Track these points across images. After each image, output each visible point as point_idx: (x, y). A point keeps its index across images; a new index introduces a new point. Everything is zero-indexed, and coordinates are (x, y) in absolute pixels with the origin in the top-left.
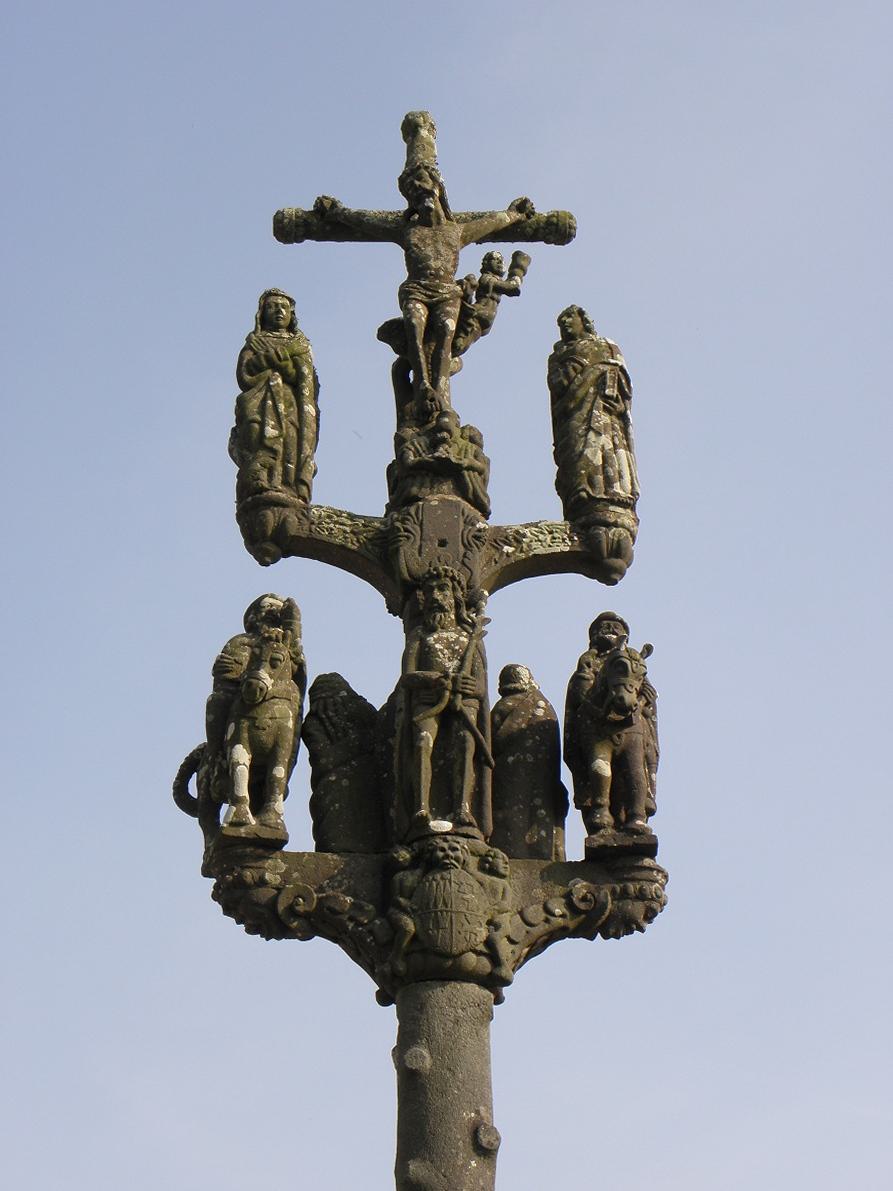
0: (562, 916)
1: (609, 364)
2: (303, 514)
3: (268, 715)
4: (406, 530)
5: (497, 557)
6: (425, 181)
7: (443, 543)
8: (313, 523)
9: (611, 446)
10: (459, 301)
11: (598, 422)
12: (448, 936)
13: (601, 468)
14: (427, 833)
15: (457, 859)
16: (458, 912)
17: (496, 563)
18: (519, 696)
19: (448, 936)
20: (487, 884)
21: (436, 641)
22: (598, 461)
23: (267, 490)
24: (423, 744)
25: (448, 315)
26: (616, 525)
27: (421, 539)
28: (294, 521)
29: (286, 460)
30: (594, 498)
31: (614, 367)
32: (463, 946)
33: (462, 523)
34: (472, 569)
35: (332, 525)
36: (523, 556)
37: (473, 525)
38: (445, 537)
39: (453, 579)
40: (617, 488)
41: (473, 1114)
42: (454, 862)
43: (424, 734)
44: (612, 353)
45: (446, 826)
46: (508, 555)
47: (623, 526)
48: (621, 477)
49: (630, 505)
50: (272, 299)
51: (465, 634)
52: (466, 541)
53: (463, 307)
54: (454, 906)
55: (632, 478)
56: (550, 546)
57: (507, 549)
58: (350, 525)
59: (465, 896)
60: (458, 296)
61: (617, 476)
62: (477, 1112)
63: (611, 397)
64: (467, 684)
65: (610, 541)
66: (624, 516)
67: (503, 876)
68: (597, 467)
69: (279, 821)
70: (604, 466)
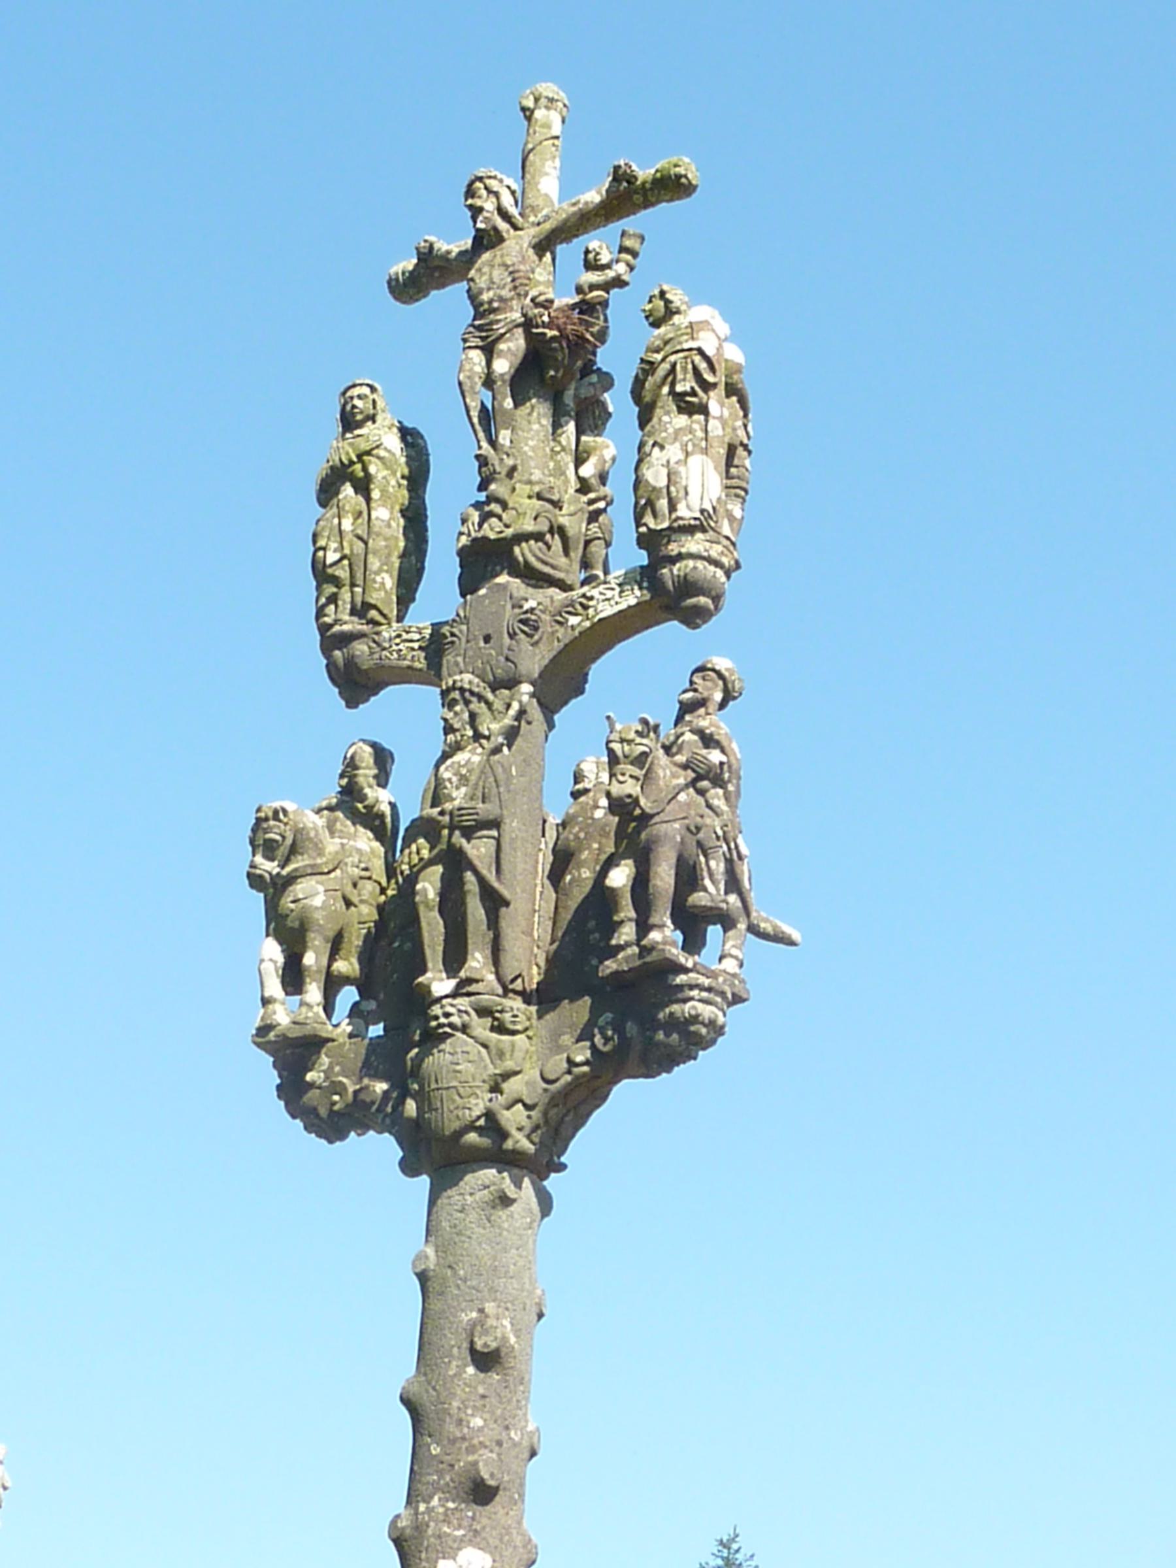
0: (587, 1063)
1: (683, 350)
2: (374, 641)
3: (291, 899)
4: (453, 635)
6: (480, 197)
7: (487, 639)
8: (384, 649)
9: (682, 456)
10: (520, 330)
11: (666, 431)
12: (439, 1119)
13: (665, 491)
14: (430, 1000)
15: (451, 1025)
16: (448, 1088)
17: (559, 641)
18: (582, 799)
19: (439, 1116)
20: (492, 1045)
21: (447, 769)
22: (662, 482)
23: (331, 626)
25: (501, 354)
26: (680, 557)
27: (468, 641)
28: (363, 652)
29: (353, 585)
30: (655, 531)
31: (686, 353)
32: (456, 1125)
33: (509, 606)
34: (515, 661)
35: (401, 647)
36: (587, 624)
37: (521, 607)
38: (490, 631)
39: (462, 690)
40: (682, 511)
41: (474, 1315)
42: (447, 1030)
43: (419, 887)
44: (692, 334)
46: (573, 627)
47: (691, 556)
49: (695, 526)
50: (349, 394)
51: (480, 750)
52: (511, 631)
53: (529, 336)
54: (444, 1081)
55: (703, 493)
56: (617, 603)
57: (574, 620)
58: (418, 641)
59: (458, 1068)
60: (518, 326)
61: (682, 493)
62: (481, 1311)
63: (685, 394)
64: (462, 815)
65: (676, 579)
69: (310, 1014)
70: (668, 487)
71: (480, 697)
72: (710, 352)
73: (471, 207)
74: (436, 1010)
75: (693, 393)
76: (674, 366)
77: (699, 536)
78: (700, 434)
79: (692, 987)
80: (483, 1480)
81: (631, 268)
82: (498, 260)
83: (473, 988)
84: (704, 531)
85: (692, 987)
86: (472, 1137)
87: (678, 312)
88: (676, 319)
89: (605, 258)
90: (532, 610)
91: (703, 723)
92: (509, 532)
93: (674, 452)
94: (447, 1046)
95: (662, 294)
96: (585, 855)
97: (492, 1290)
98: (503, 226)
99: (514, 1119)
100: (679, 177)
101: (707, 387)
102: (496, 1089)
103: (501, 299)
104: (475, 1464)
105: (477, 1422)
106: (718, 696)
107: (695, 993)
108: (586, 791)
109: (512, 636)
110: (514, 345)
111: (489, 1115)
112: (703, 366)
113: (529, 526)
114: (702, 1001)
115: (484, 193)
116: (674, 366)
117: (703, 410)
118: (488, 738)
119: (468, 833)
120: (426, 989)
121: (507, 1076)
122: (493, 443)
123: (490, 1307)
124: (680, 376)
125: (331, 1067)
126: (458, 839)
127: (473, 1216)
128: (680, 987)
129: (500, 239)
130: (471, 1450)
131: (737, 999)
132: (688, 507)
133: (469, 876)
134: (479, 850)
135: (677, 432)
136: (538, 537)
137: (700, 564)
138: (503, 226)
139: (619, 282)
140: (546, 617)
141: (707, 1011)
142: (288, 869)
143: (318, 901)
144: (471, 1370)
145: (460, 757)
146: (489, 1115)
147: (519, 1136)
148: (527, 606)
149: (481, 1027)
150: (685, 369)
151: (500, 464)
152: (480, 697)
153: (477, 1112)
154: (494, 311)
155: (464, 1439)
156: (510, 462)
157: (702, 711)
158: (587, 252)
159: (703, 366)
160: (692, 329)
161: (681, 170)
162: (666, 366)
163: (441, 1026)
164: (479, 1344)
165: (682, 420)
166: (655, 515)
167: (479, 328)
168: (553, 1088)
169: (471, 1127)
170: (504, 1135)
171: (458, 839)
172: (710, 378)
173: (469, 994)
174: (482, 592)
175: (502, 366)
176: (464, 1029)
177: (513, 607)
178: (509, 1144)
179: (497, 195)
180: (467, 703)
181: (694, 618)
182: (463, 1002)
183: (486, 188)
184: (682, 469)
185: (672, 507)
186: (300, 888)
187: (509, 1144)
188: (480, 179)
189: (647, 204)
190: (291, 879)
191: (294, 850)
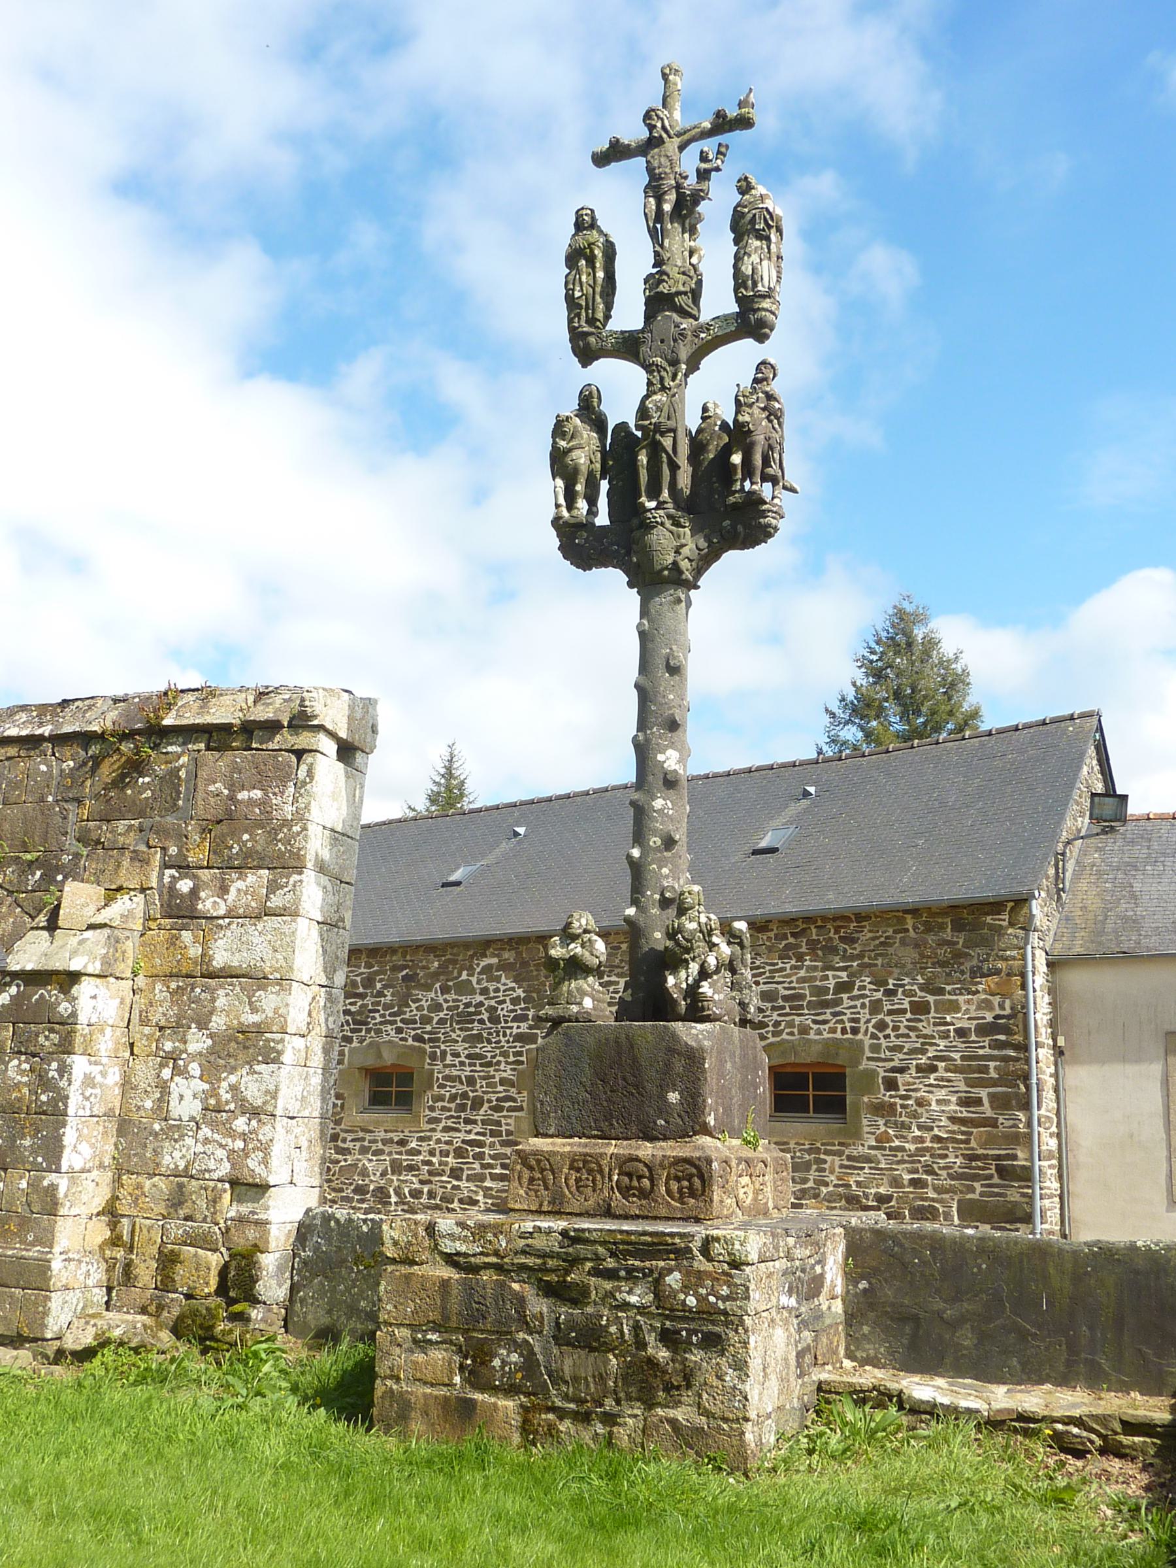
5: (696, 341)
7: (662, 341)
9: (758, 260)
15: (657, 522)
22: (749, 272)
24: (639, 463)
25: (666, 201)
26: (759, 309)
32: (660, 567)
39: (657, 365)
40: (760, 288)
45: (652, 504)
48: (762, 279)
53: (678, 193)
57: (703, 335)
62: (671, 649)
63: (760, 230)
66: (766, 304)
67: (685, 527)
68: (748, 276)
70: (752, 275)
71: (665, 369)
72: (771, 210)
73: (646, 125)
74: (648, 514)
75: (764, 230)
76: (754, 215)
77: (768, 300)
78: (766, 250)
79: (769, 511)
80: (676, 721)
81: (723, 162)
82: (663, 153)
83: (665, 506)
84: (770, 297)
85: (769, 511)
86: (666, 573)
87: (753, 188)
88: (753, 192)
89: (711, 157)
90: (685, 329)
91: (768, 389)
92: (673, 290)
93: (755, 258)
94: (655, 531)
95: (746, 178)
96: (711, 447)
97: (675, 640)
98: (665, 136)
99: (685, 565)
100: (749, 119)
101: (770, 227)
102: (677, 552)
103: (665, 173)
104: (673, 714)
105: (671, 697)
106: (771, 376)
107: (770, 514)
108: (710, 417)
109: (675, 340)
110: (672, 197)
111: (675, 563)
112: (768, 217)
113: (682, 289)
114: (773, 518)
115: (655, 118)
116: (754, 215)
117: (768, 239)
118: (670, 389)
119: (663, 434)
120: (642, 504)
121: (683, 546)
122: (662, 246)
123: (674, 647)
124: (758, 221)
125: (587, 537)
126: (658, 437)
127: (666, 608)
128: (764, 511)
129: (663, 142)
130: (669, 708)
131: (783, 517)
132: (763, 286)
133: (664, 455)
134: (667, 442)
135: (756, 248)
136: (685, 293)
137: (768, 314)
138: (665, 136)
139: (718, 169)
140: (690, 333)
141: (774, 522)
142: (571, 444)
143: (582, 461)
144: (667, 675)
145: (655, 397)
146: (675, 563)
147: (687, 573)
148: (682, 327)
149: (668, 523)
150: (760, 218)
151: (666, 255)
152: (665, 369)
153: (670, 562)
154: (662, 179)
155: (666, 703)
156: (668, 255)
157: (765, 383)
158: (702, 152)
159: (768, 217)
160: (762, 198)
161: (750, 115)
162: (750, 215)
163: (652, 522)
164: (672, 663)
165: (758, 243)
166: (746, 289)
167: (655, 187)
168: (702, 553)
169: (666, 568)
170: (681, 572)
171: (658, 437)
172: (770, 222)
173: (664, 509)
174: (659, 318)
175: (667, 207)
176: (662, 524)
177: (675, 327)
178: (684, 577)
179: (662, 119)
180: (659, 372)
181: (761, 338)
182: (661, 512)
183: (657, 115)
184: (759, 267)
185: (755, 284)
186: (575, 454)
187: (684, 577)
188: (653, 110)
189: (730, 130)
190: (570, 450)
191: (572, 437)
